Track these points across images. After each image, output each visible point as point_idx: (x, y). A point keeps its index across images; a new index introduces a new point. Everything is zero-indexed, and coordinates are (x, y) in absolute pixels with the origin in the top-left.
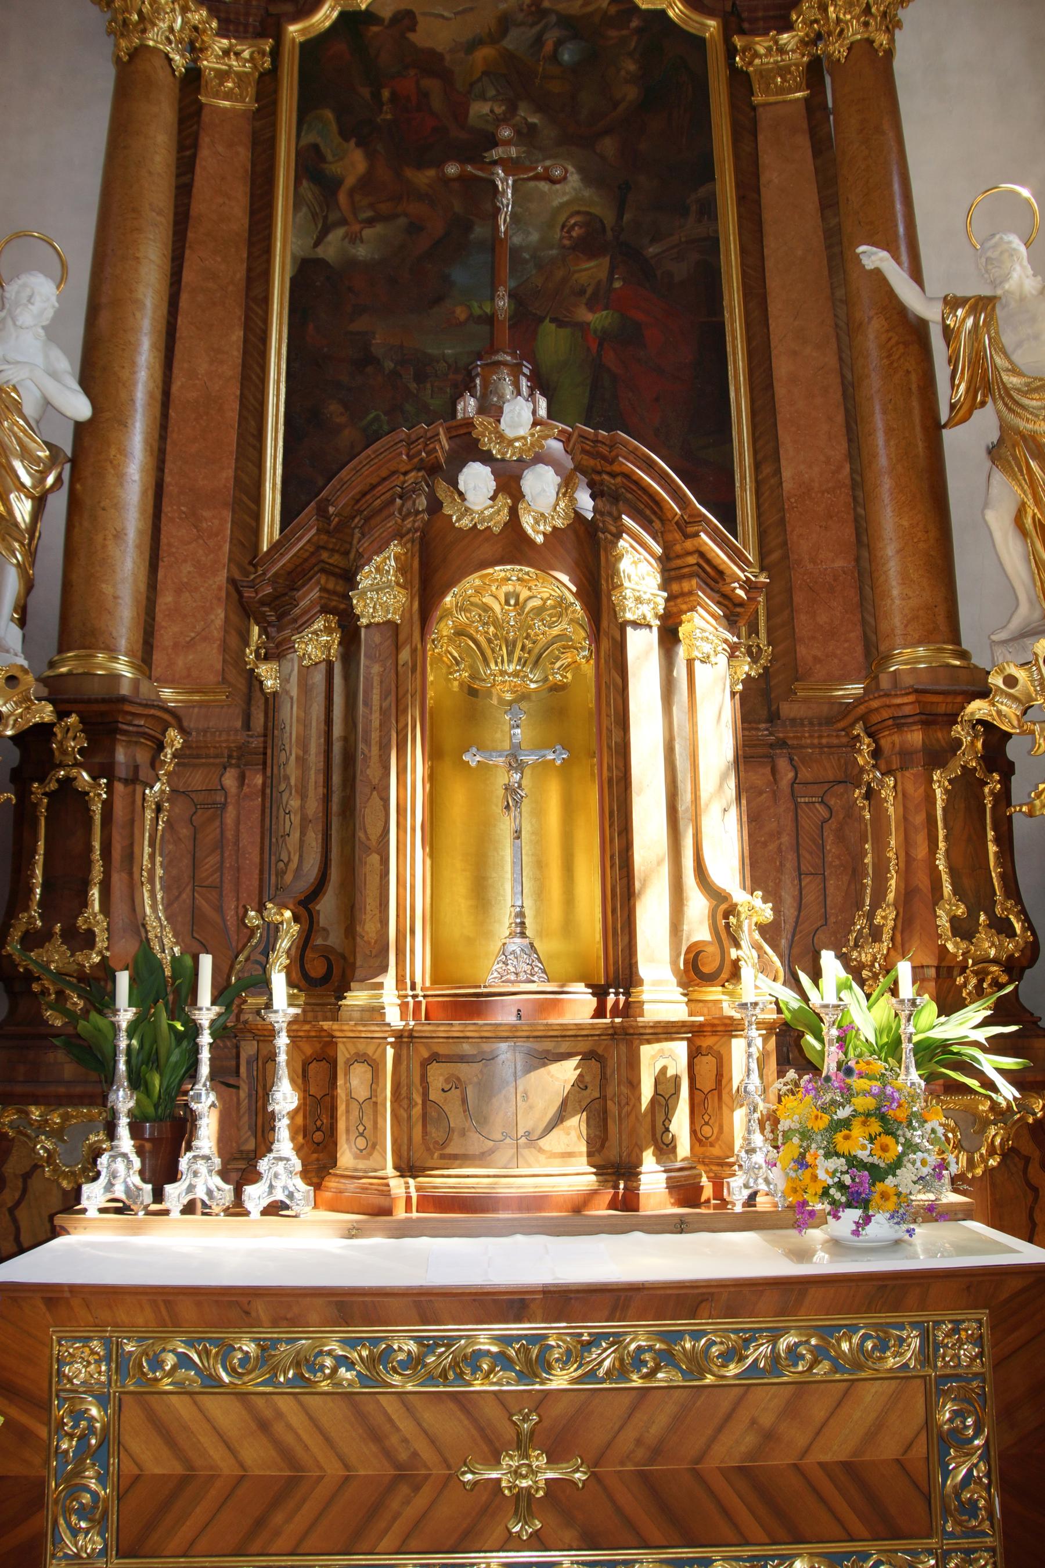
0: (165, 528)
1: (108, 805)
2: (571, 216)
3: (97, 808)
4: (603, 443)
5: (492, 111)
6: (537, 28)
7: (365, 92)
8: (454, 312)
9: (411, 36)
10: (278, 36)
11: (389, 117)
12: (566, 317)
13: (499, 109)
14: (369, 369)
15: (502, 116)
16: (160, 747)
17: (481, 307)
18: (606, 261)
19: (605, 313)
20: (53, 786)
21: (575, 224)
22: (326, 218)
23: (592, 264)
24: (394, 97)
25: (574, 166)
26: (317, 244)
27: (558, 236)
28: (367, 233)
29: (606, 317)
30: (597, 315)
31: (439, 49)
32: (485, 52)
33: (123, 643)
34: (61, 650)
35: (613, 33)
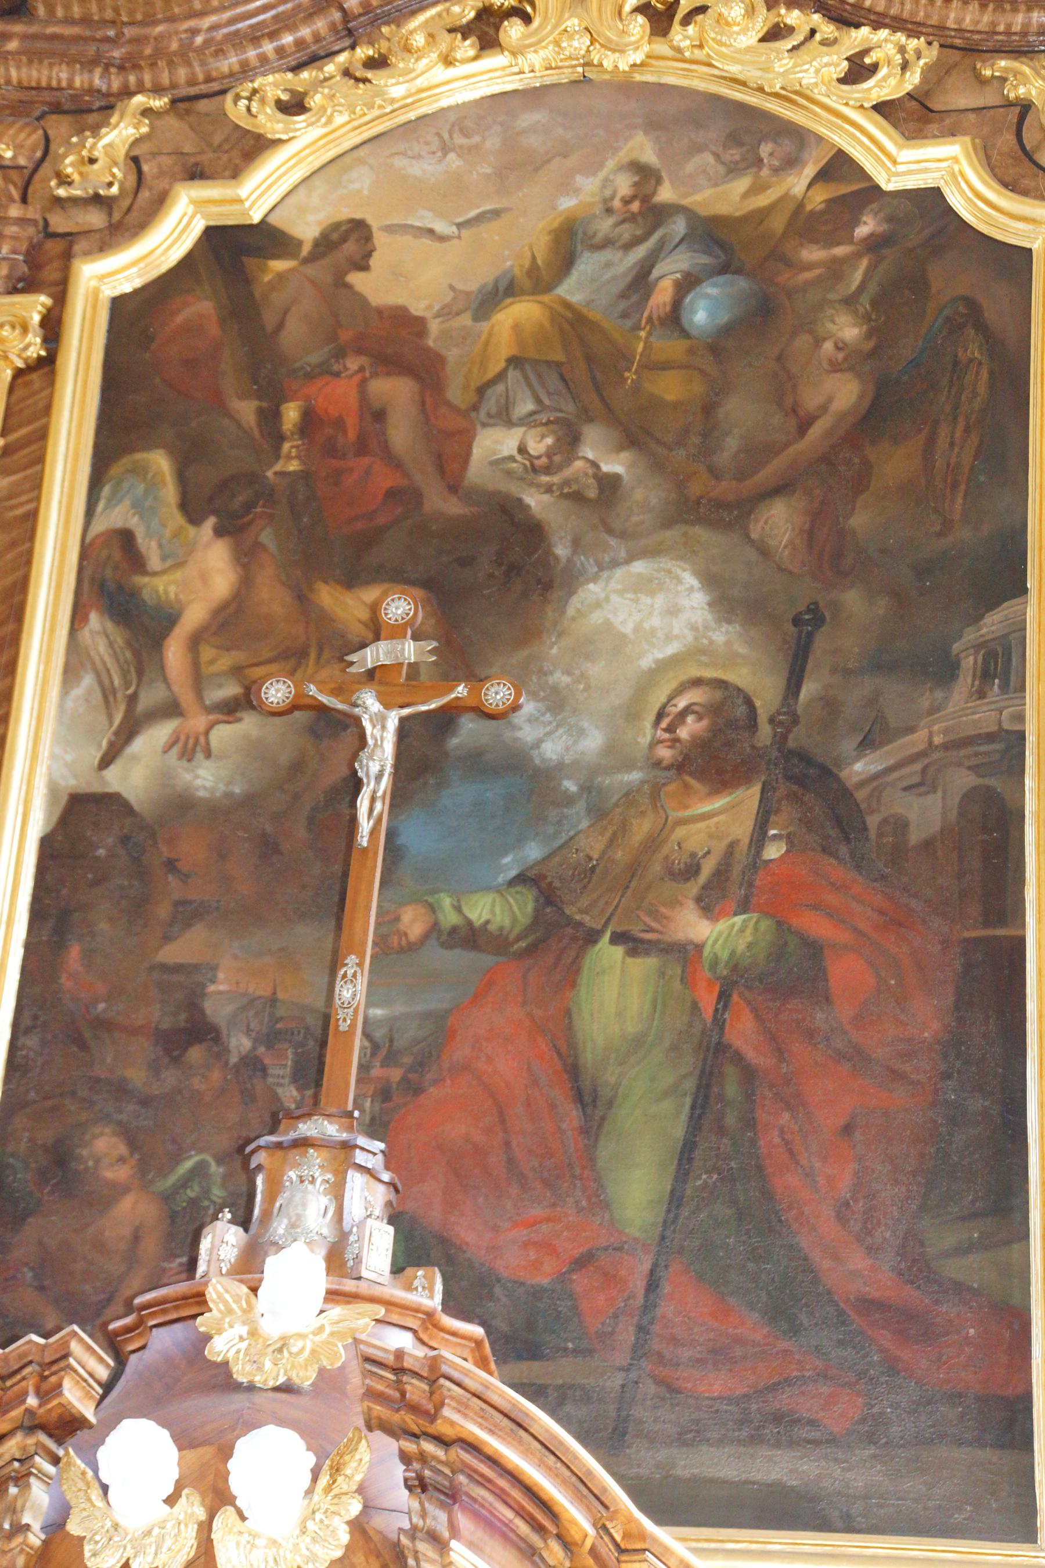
2: (679, 691)
4: (416, 1374)
5: (522, 450)
6: (640, 252)
7: (246, 410)
8: (397, 919)
9: (356, 279)
11: (294, 466)
12: (652, 930)
13: (539, 444)
14: (195, 1054)
15: (544, 460)
17: (458, 909)
18: (750, 796)
19: (739, 919)
22: (133, 699)
23: (719, 802)
24: (309, 422)
25: (697, 574)
26: (106, 762)
27: (645, 740)
28: (223, 735)
29: (742, 930)
30: (722, 925)
31: (417, 309)
35: (812, 254)
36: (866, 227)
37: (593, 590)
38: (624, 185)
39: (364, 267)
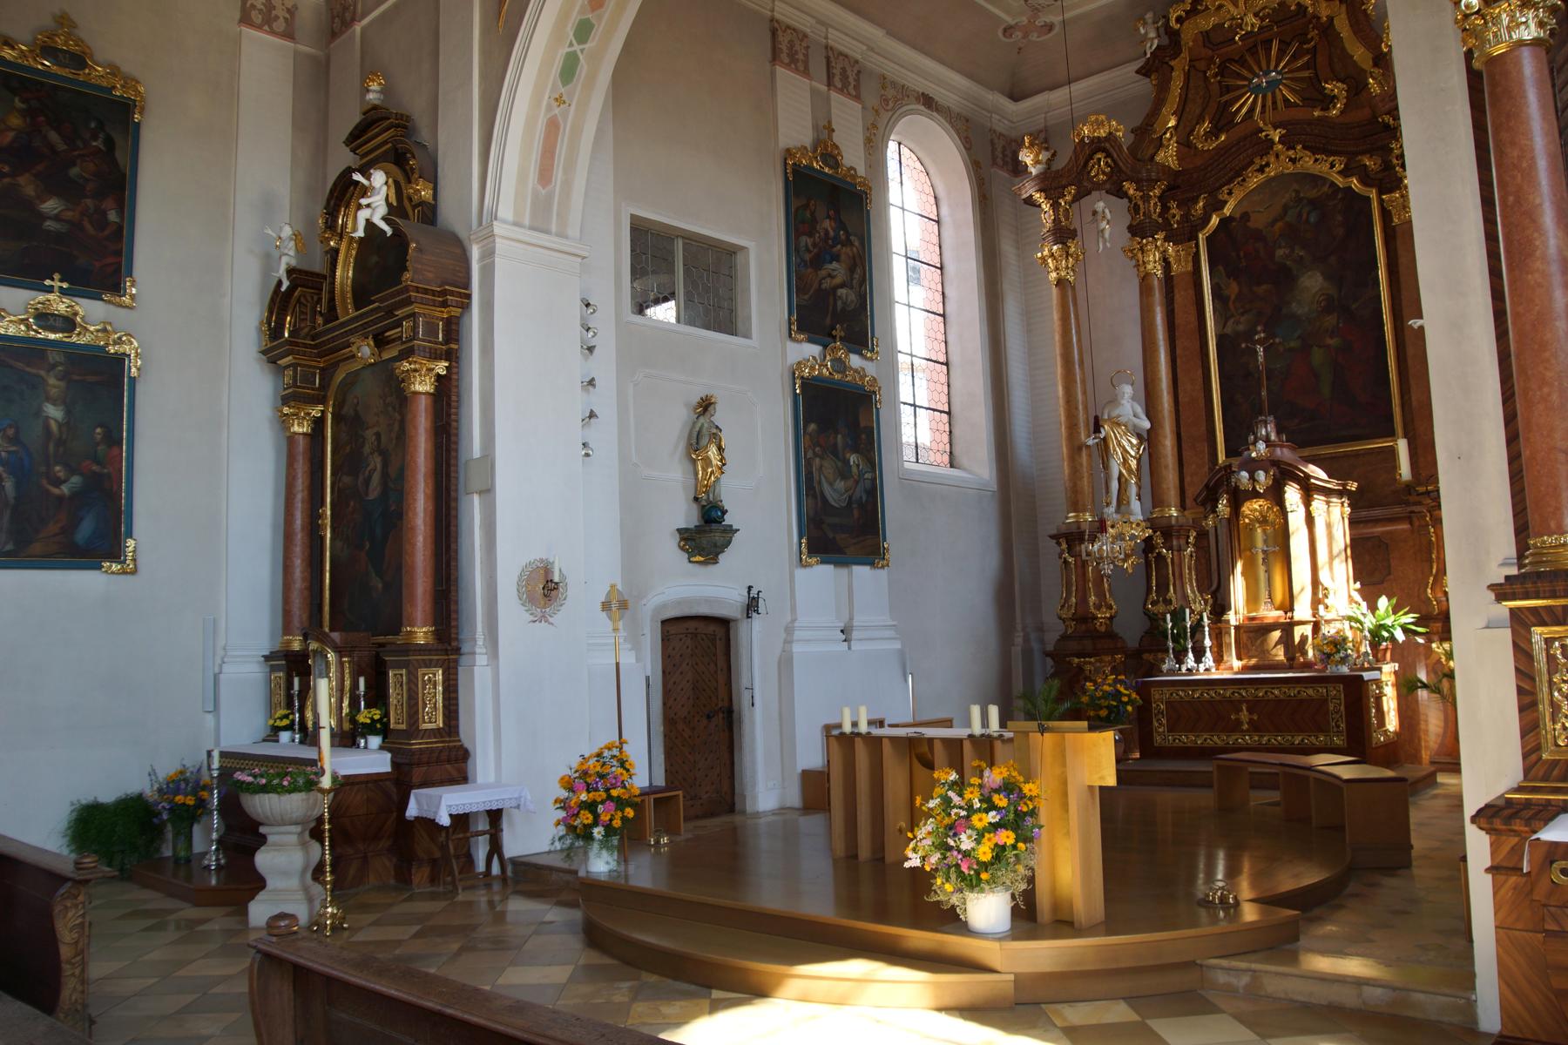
0: (1184, 453)
1: (1172, 559)
3: (1169, 560)
6: (1299, 208)
9: (1248, 224)
10: (1197, 239)
13: (1287, 252)
16: (1188, 537)
20: (1155, 555)
21: (1323, 300)
26: (1224, 327)
28: (1242, 319)
32: (1279, 225)
33: (1173, 503)
34: (1154, 508)
36: (1340, 196)
37: (1302, 279)
38: (1294, 194)
39: (1249, 221)
